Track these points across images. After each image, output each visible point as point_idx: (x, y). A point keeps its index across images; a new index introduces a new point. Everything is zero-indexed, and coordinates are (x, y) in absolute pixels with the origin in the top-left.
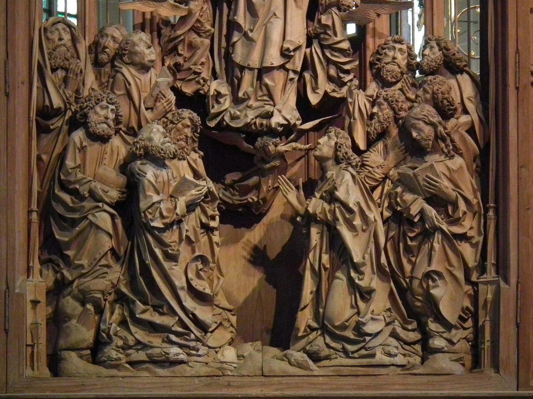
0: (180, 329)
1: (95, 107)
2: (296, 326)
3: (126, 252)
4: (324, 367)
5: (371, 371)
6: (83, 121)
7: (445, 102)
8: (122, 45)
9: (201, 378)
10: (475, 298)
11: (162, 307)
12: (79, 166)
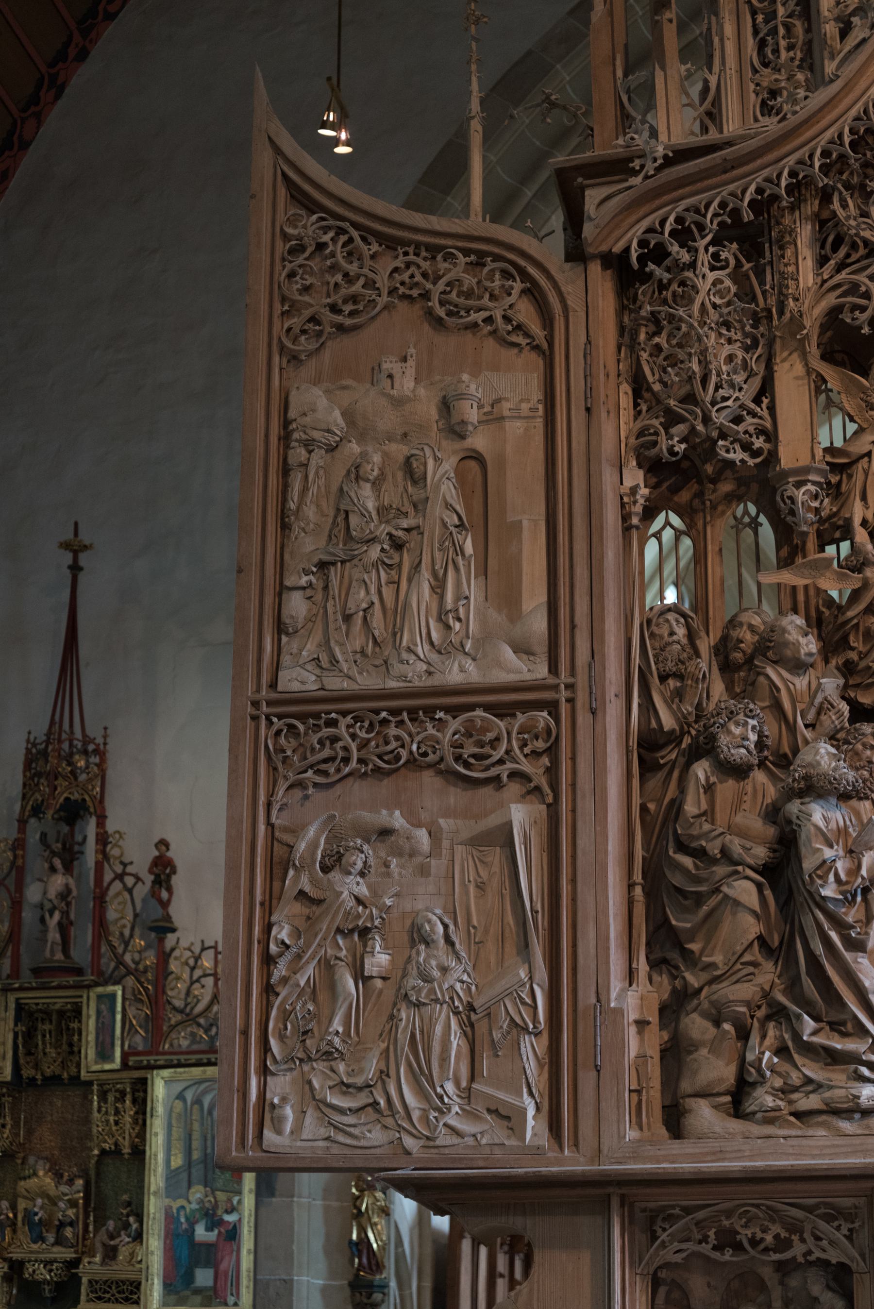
3: (781, 943)
6: (709, 746)
8: (765, 635)
12: (704, 814)
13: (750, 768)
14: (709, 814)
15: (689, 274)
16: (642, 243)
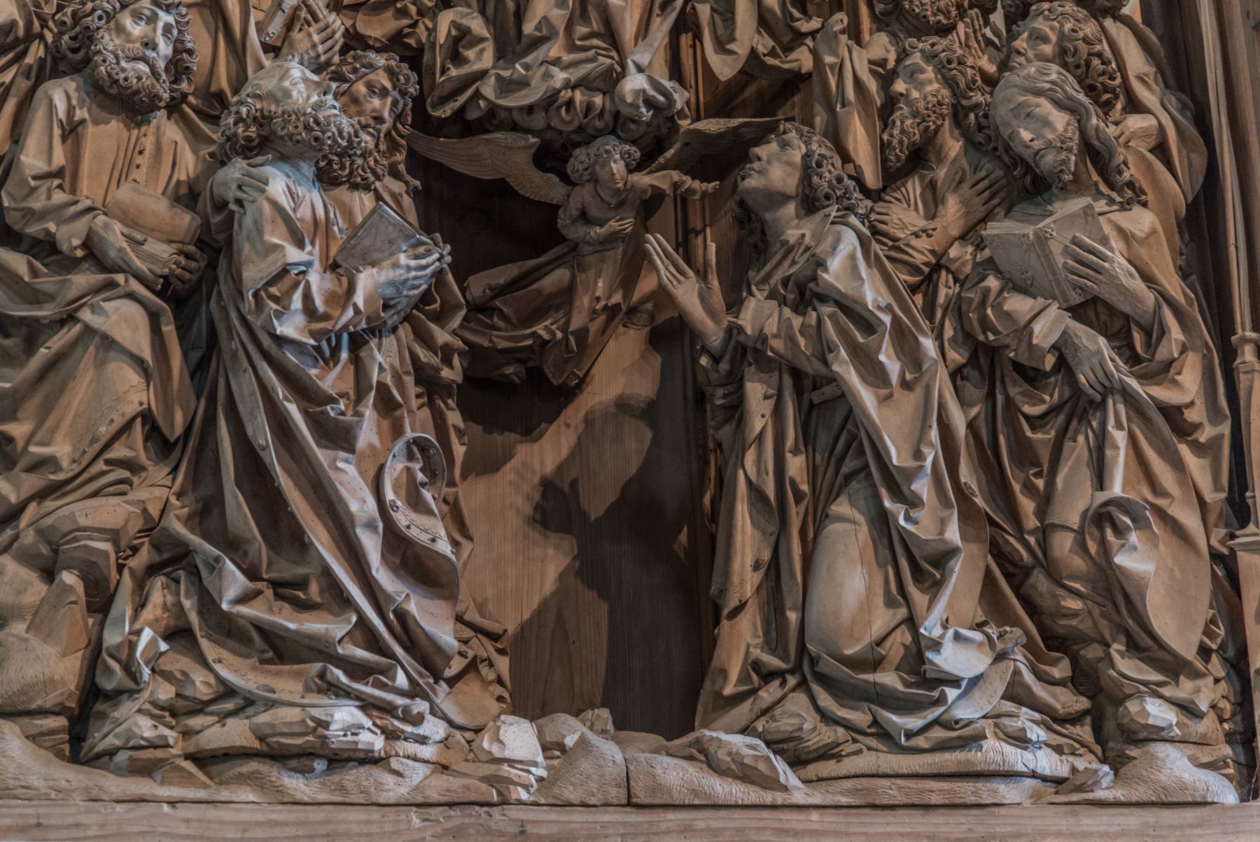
0: (360, 653)
1: (118, 16)
2: (715, 663)
4: (820, 780)
5: (967, 791)
6: (79, 56)
7: (1096, 62)
9: (434, 812)
11: (302, 584)
12: (59, 173)
13: (153, 108)
14: (66, 176)
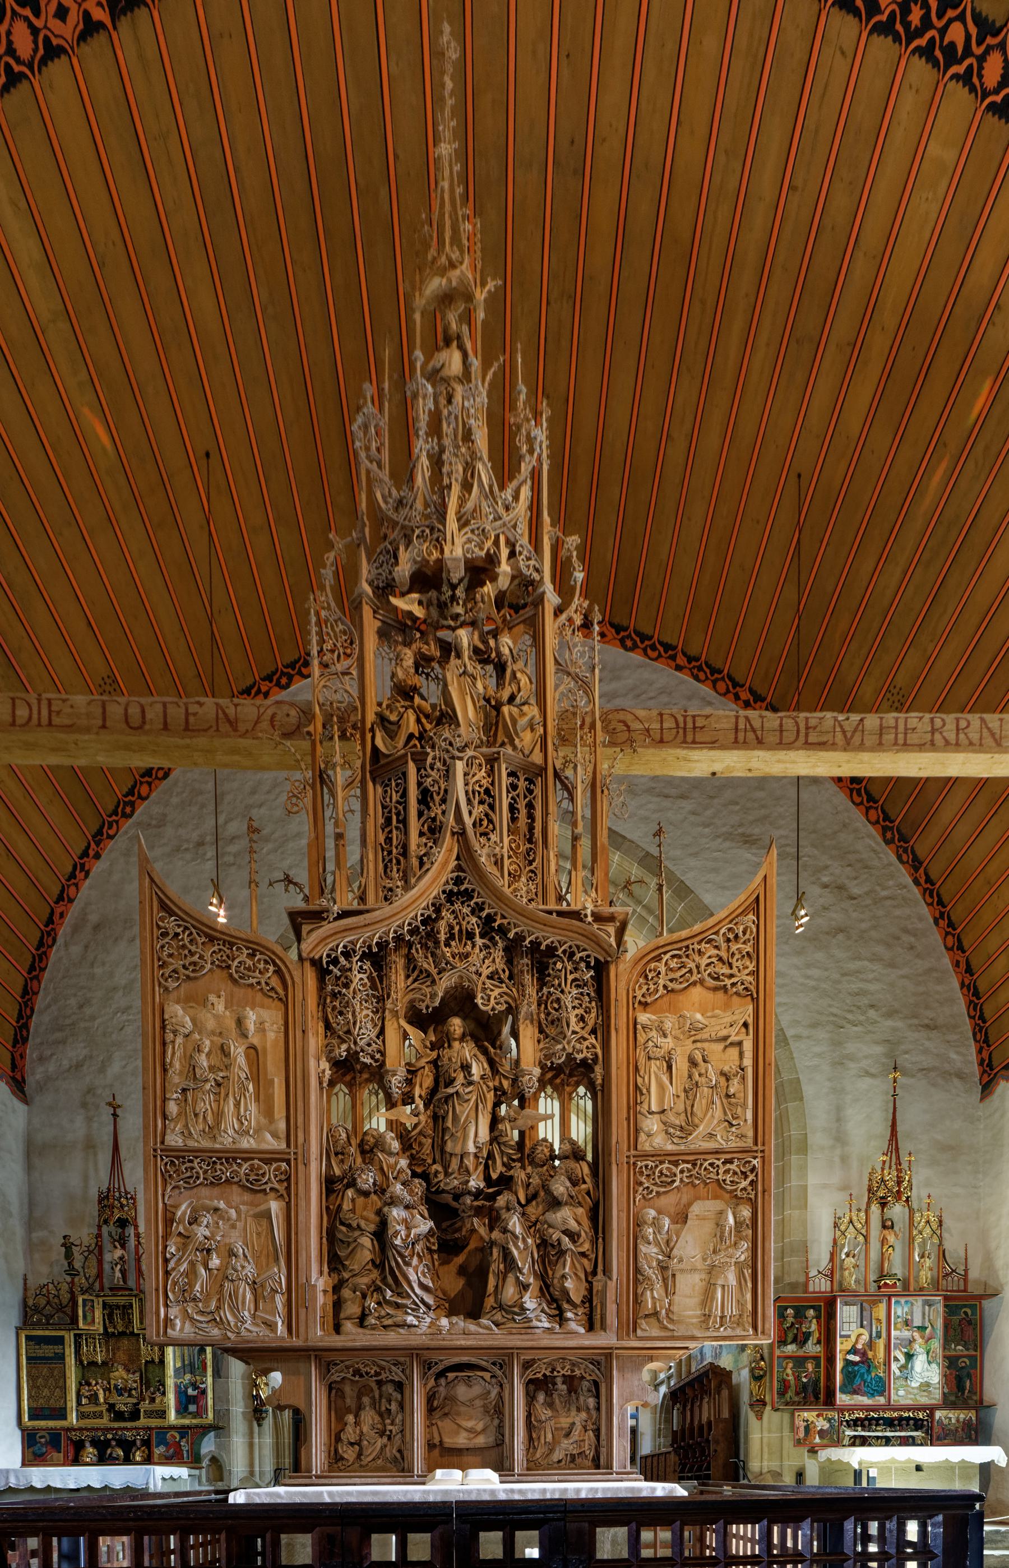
10: (590, 1290)
15: (349, 973)
16: (329, 956)
